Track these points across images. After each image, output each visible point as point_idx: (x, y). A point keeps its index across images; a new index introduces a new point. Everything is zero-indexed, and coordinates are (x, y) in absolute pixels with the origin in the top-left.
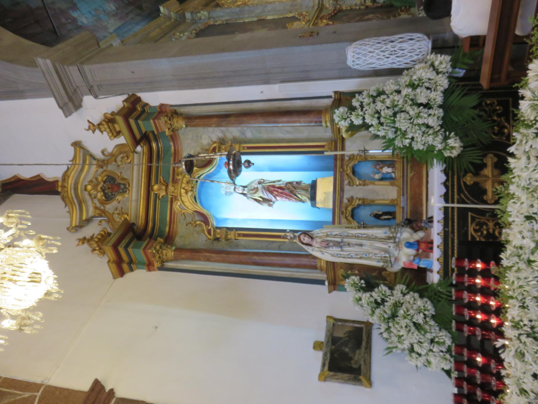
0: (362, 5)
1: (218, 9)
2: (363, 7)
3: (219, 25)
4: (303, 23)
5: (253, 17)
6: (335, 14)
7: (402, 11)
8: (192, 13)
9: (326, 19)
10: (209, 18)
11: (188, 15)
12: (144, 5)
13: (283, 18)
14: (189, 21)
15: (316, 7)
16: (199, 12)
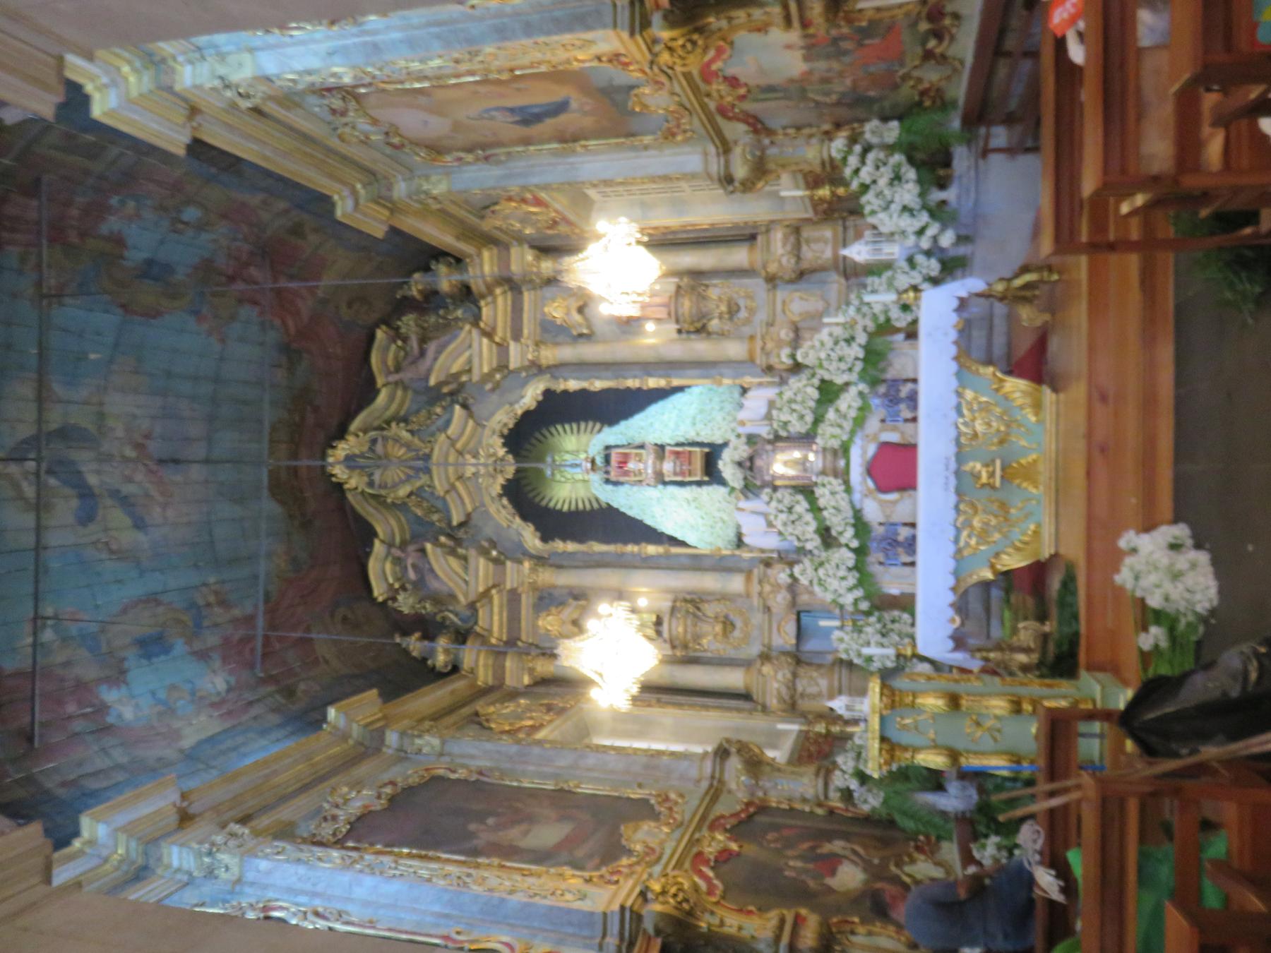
0: (820, 805)
1: (472, 730)
2: (820, 811)
3: (458, 781)
4: (666, 830)
5: (545, 776)
6: (750, 817)
7: (919, 849)
8: (403, 734)
9: (726, 830)
10: (441, 754)
11: (392, 738)
12: (302, 686)
13: (619, 798)
14: (390, 751)
15: (705, 784)
16: (419, 736)
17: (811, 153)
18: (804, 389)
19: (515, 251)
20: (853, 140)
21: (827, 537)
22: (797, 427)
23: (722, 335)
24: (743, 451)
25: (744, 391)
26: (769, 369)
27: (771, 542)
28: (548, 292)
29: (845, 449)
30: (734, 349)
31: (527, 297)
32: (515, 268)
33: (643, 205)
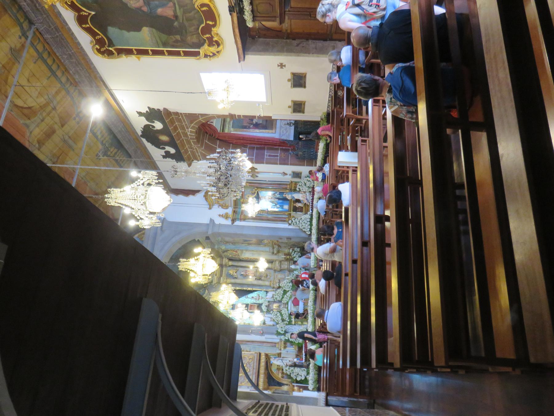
17: (286, 251)
18: (280, 291)
19: (224, 259)
20: (293, 250)
21: (283, 320)
22: (279, 299)
23: (264, 280)
24: (267, 304)
25: (267, 292)
26: (274, 288)
27: (272, 323)
28: (229, 268)
29: (287, 303)
30: (267, 283)
31: (224, 269)
32: (224, 263)
33: (253, 254)
